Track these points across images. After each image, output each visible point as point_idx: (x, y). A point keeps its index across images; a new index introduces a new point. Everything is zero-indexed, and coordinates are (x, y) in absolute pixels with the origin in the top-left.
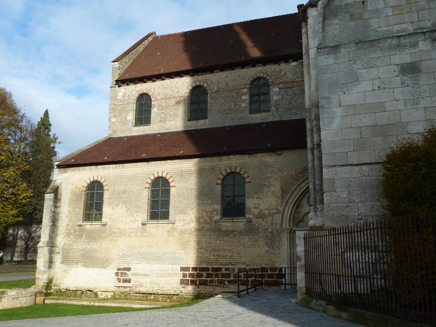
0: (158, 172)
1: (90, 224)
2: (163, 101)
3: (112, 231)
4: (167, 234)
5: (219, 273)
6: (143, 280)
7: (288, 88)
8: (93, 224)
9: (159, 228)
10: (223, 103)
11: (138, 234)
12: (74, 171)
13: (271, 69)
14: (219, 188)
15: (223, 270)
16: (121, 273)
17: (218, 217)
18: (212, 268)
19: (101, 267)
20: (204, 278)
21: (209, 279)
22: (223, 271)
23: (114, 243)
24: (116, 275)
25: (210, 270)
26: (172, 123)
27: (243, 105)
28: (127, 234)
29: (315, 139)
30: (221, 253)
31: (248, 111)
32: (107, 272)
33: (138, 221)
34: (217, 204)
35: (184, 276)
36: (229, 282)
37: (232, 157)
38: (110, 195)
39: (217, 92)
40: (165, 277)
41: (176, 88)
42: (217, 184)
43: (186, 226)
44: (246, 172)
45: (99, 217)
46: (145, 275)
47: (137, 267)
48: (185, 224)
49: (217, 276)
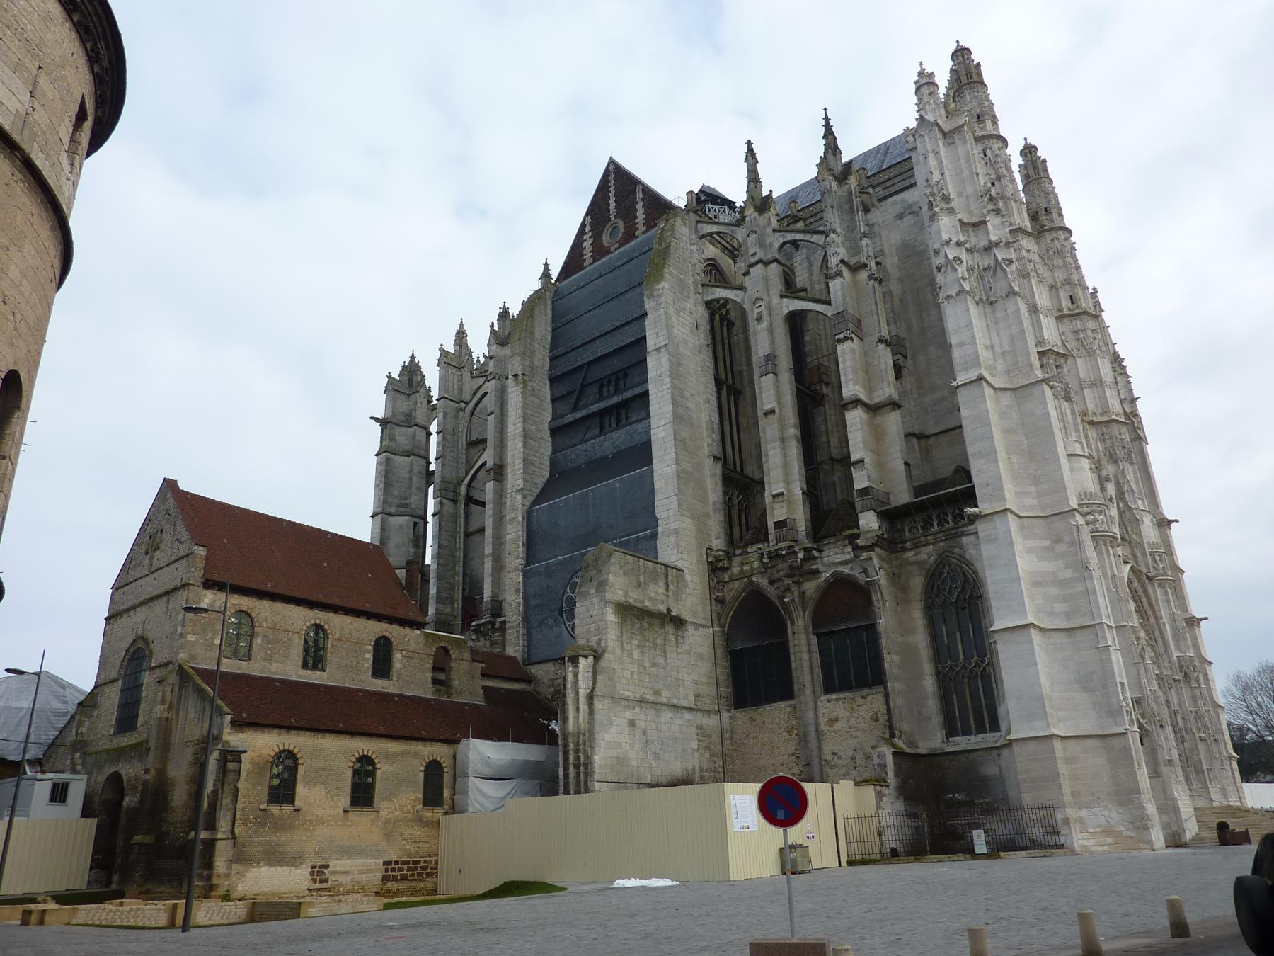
14: (422, 775)
27: (366, 665)
29: (582, 759)
35: (387, 870)
39: (339, 639)
45: (290, 799)
46: (346, 873)
47: (336, 864)
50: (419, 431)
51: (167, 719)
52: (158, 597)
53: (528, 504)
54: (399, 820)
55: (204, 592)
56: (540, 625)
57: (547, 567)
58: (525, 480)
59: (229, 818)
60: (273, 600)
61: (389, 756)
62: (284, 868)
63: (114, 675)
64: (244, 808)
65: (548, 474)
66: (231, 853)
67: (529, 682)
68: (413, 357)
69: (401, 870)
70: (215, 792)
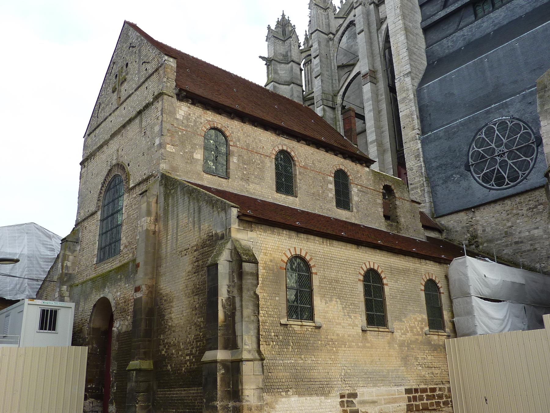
1: (300, 323)
2: (245, 152)
4: (387, 345)
8: (304, 323)
9: (377, 338)
10: (311, 185)
12: (265, 231)
14: (423, 294)
15: (438, 389)
16: (347, 401)
17: (427, 329)
20: (425, 401)
21: (429, 402)
22: (438, 392)
23: (333, 357)
24: (340, 405)
25: (429, 390)
26: (258, 187)
28: (347, 343)
31: (334, 204)
32: (329, 401)
33: (357, 326)
35: (409, 400)
39: (305, 168)
40: (392, 403)
41: (260, 141)
43: (403, 336)
46: (374, 402)
48: (402, 334)
50: (295, 65)
51: (154, 232)
52: (130, 121)
53: (416, 84)
54: (412, 342)
55: (178, 103)
56: (445, 182)
57: (446, 131)
58: (411, 65)
59: (253, 332)
60: (243, 121)
62: (315, 398)
63: (93, 209)
65: (426, 63)
66: (260, 379)
67: (440, 231)
68: (283, 15)
70: (231, 301)
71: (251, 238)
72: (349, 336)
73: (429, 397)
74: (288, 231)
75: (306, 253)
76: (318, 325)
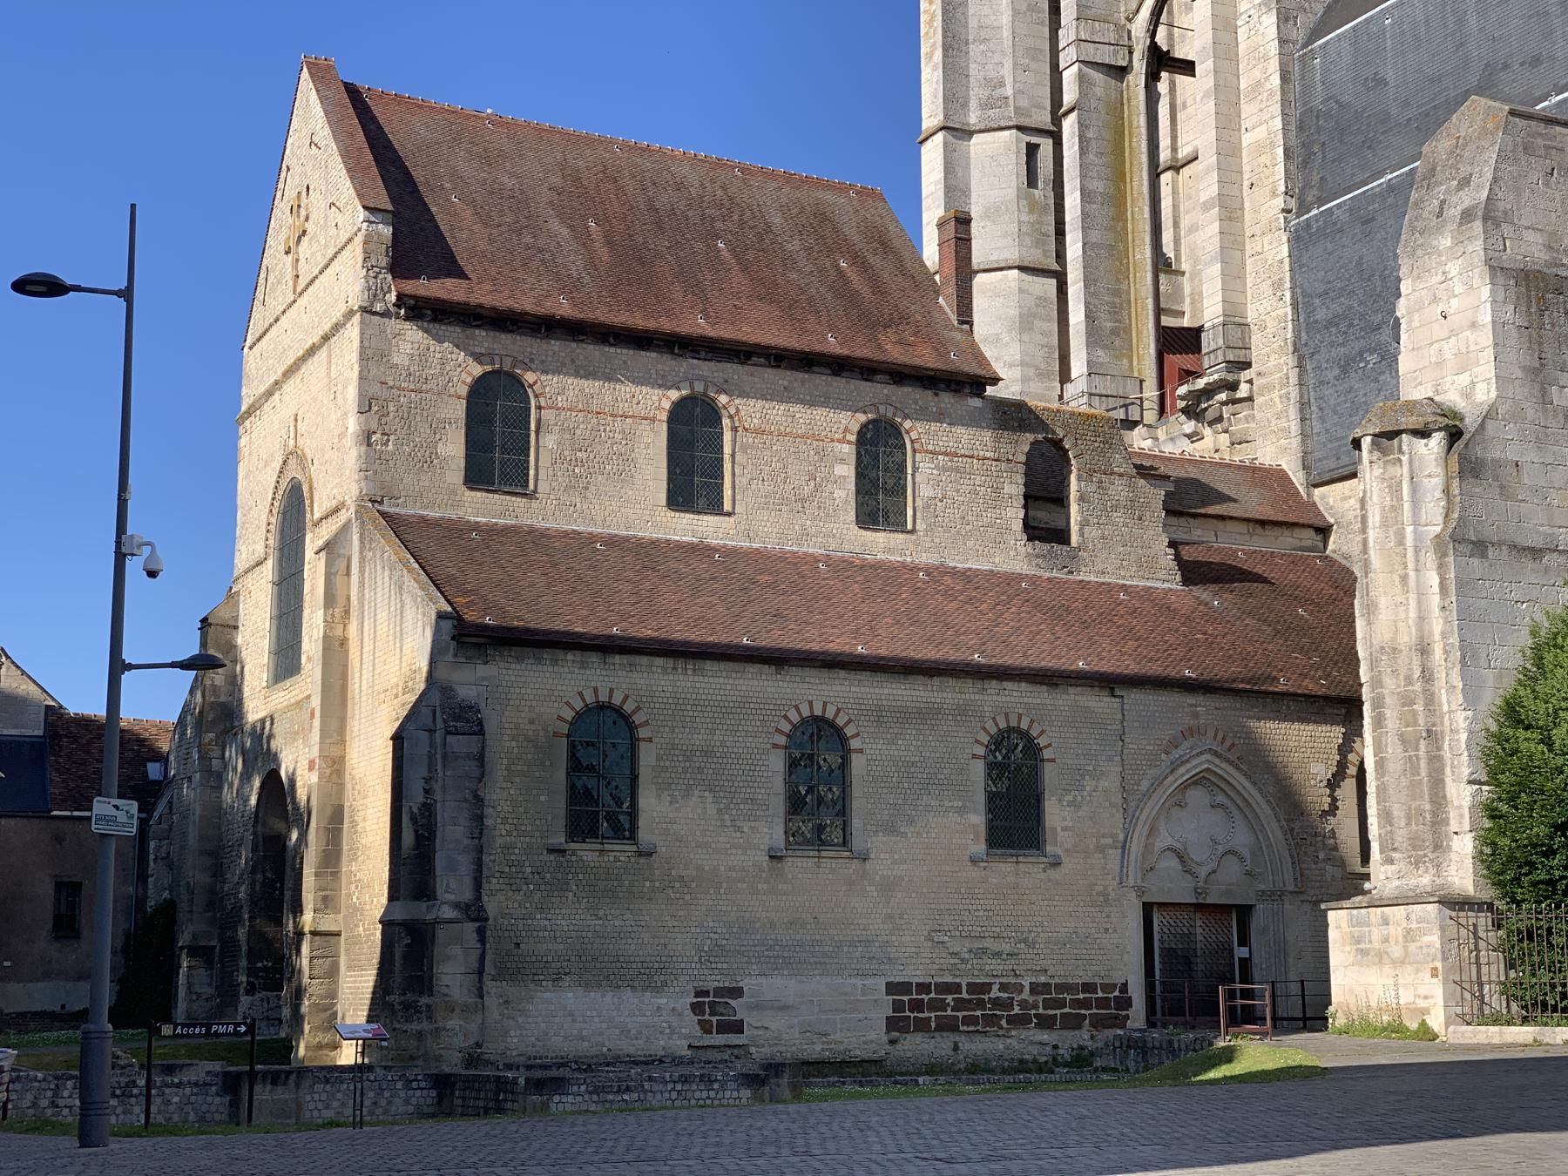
0: (810, 703)
3: (674, 872)
5: (986, 997)
6: (776, 1023)
7: (957, 470)
11: (760, 886)
12: (519, 660)
13: (916, 402)
15: (995, 988)
17: (981, 847)
18: (968, 984)
19: (645, 989)
21: (960, 1014)
22: (995, 993)
24: (693, 1010)
30: (988, 943)
34: (975, 811)
35: (898, 1006)
36: (1012, 1020)
37: (1008, 685)
38: (659, 758)
40: (844, 1011)
42: (974, 756)
44: (1043, 732)
45: (625, 827)
46: (784, 1008)
48: (894, 862)
49: (981, 1004)
52: (312, 351)
53: (1298, 34)
56: (1345, 371)
61: (879, 715)
62: (627, 994)
64: (508, 848)
69: (939, 1005)
71: (483, 679)
72: (731, 869)
73: (960, 1004)
74: (578, 653)
75: (626, 698)
76: (644, 848)
